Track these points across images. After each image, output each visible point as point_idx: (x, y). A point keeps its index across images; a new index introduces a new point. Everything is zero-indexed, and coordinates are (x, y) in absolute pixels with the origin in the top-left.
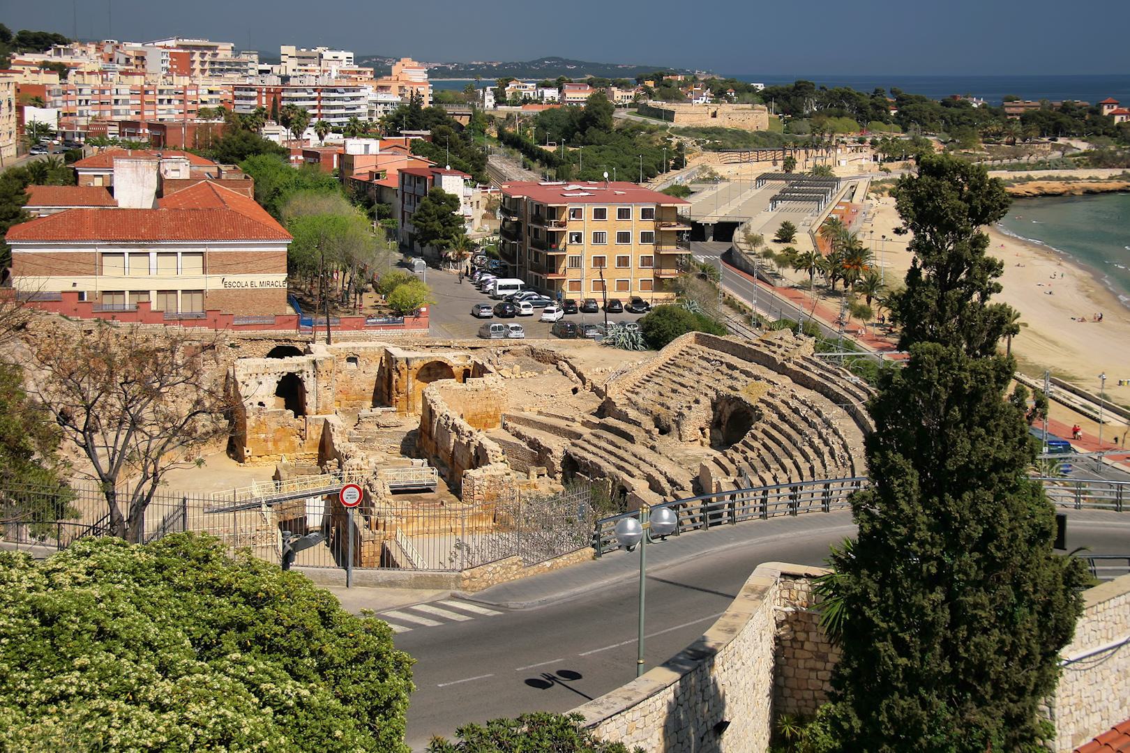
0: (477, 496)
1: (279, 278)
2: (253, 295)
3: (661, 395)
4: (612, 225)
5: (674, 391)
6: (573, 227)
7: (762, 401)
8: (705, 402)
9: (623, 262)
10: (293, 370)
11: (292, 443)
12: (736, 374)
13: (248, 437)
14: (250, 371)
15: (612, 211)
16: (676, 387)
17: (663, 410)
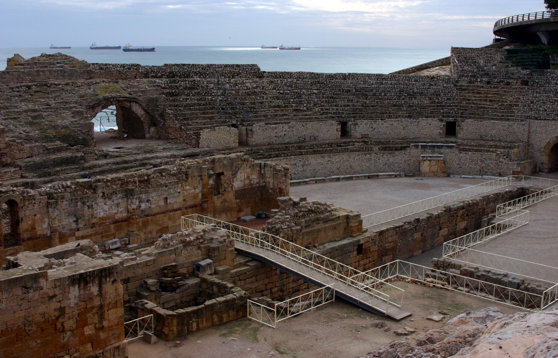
5: (35, 118)
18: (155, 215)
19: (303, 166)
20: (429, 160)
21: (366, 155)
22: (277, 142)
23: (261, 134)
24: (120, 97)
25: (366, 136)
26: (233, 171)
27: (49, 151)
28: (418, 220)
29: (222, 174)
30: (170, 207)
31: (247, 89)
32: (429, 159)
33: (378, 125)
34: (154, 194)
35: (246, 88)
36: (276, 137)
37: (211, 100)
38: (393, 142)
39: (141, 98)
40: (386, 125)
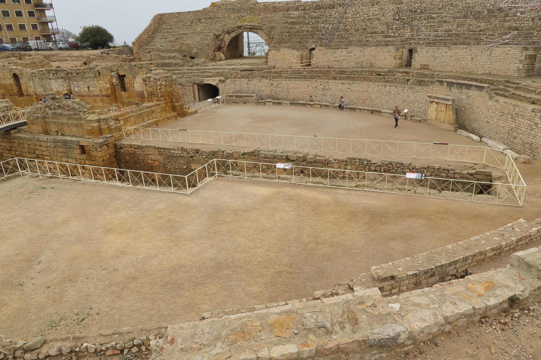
9: (22, 27)
18: (84, 96)
19: (323, 90)
20: (437, 103)
21: (385, 86)
22: (336, 67)
23: (322, 57)
25: (427, 67)
26: (132, 75)
27: (163, 58)
28: (197, 151)
29: (125, 76)
30: (92, 94)
32: (436, 100)
33: (441, 53)
34: (81, 83)
35: (366, 16)
37: (324, 28)
38: (437, 75)
39: (264, 26)
40: (450, 53)
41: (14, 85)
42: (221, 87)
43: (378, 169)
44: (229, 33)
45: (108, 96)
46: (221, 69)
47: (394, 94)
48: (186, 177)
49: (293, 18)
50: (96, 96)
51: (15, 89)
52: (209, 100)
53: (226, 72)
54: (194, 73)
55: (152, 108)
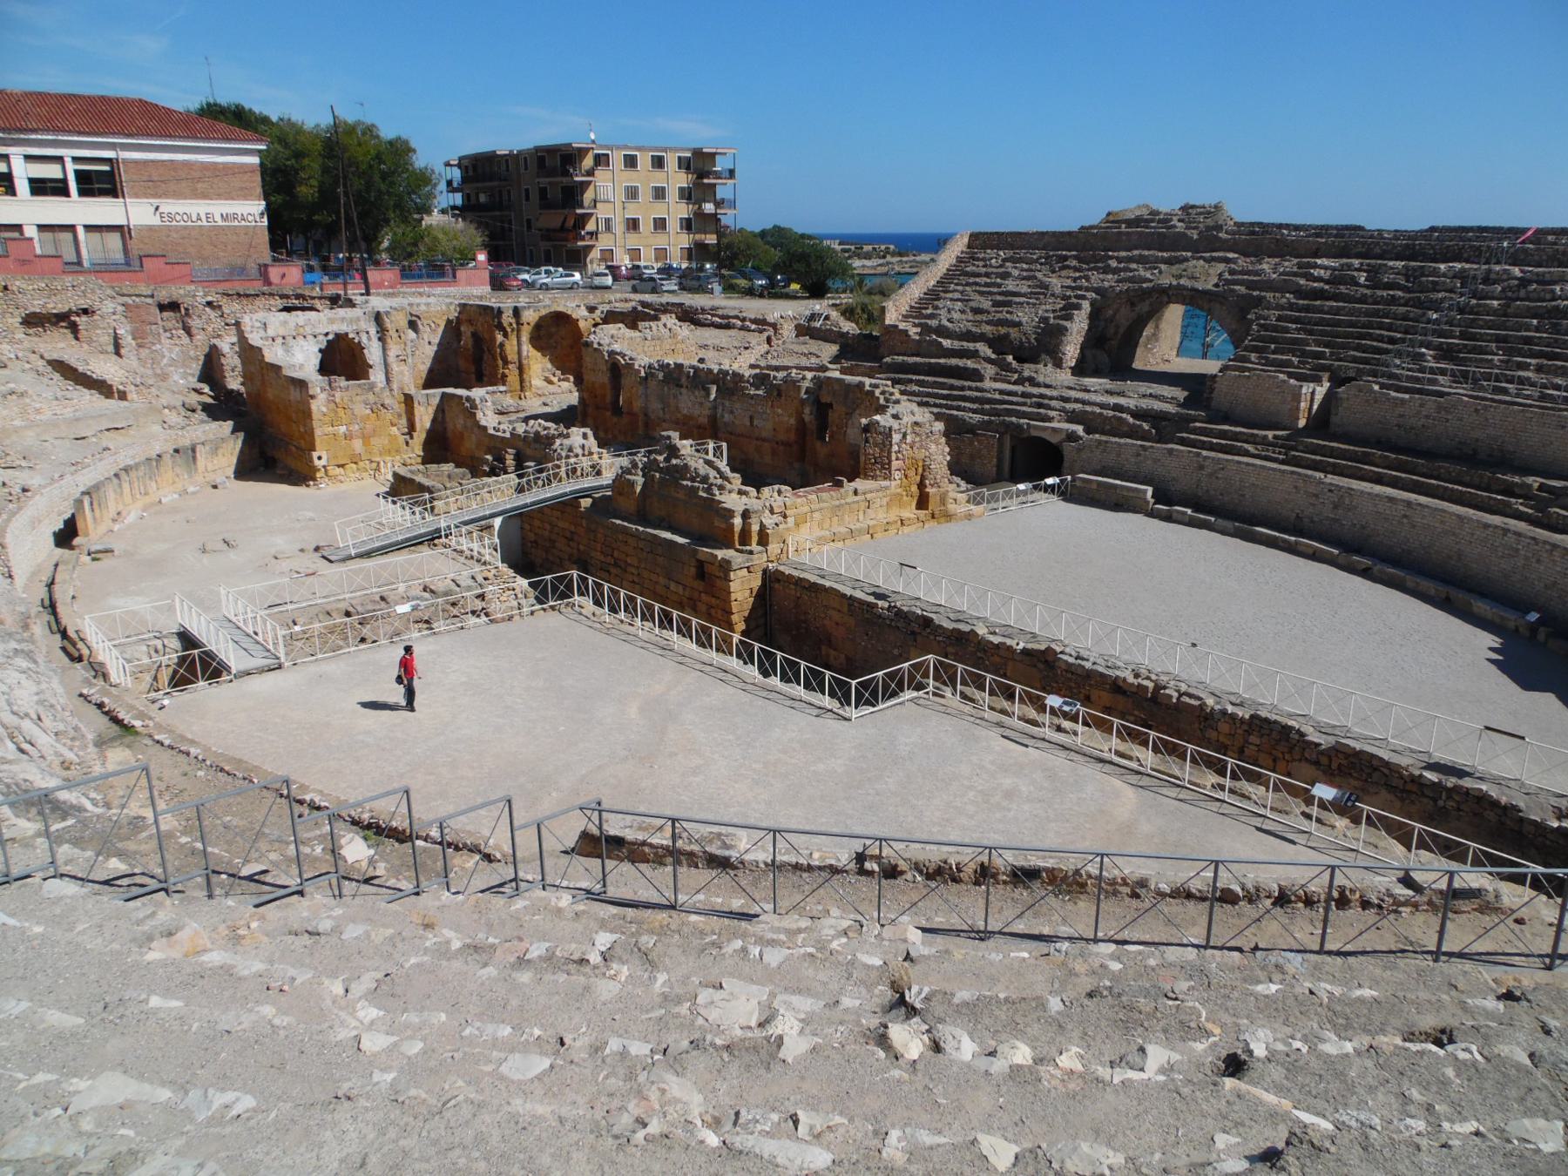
0: (895, 464)
1: (252, 210)
2: (214, 234)
3: (977, 311)
4: (644, 177)
6: (602, 178)
7: (1228, 282)
8: (1086, 305)
10: (342, 328)
11: (392, 438)
12: (1113, 263)
13: (318, 432)
14: (271, 332)
15: (644, 160)
16: (999, 298)
17: (1003, 330)
19: (1336, 507)
24: (1184, 288)
29: (831, 406)
31: (1554, 299)
34: (738, 405)
36: (1398, 426)
41: (609, 387)
42: (1068, 448)
43: (1324, 760)
44: (1133, 304)
45: (787, 444)
46: (1084, 402)
47: (1527, 558)
48: (854, 683)
49: (1319, 279)
50: (764, 440)
51: (609, 399)
52: (1022, 487)
53: (1093, 413)
54: (1012, 403)
55: (869, 496)
